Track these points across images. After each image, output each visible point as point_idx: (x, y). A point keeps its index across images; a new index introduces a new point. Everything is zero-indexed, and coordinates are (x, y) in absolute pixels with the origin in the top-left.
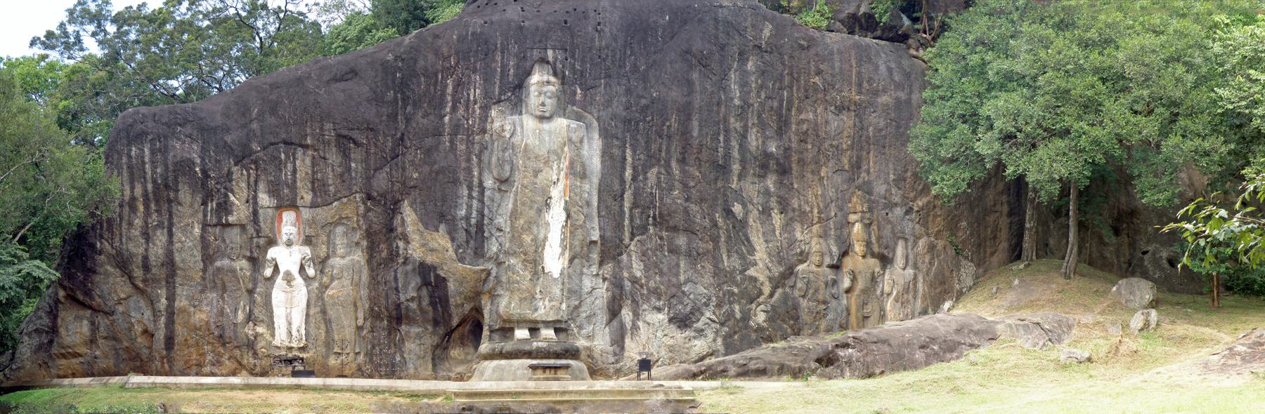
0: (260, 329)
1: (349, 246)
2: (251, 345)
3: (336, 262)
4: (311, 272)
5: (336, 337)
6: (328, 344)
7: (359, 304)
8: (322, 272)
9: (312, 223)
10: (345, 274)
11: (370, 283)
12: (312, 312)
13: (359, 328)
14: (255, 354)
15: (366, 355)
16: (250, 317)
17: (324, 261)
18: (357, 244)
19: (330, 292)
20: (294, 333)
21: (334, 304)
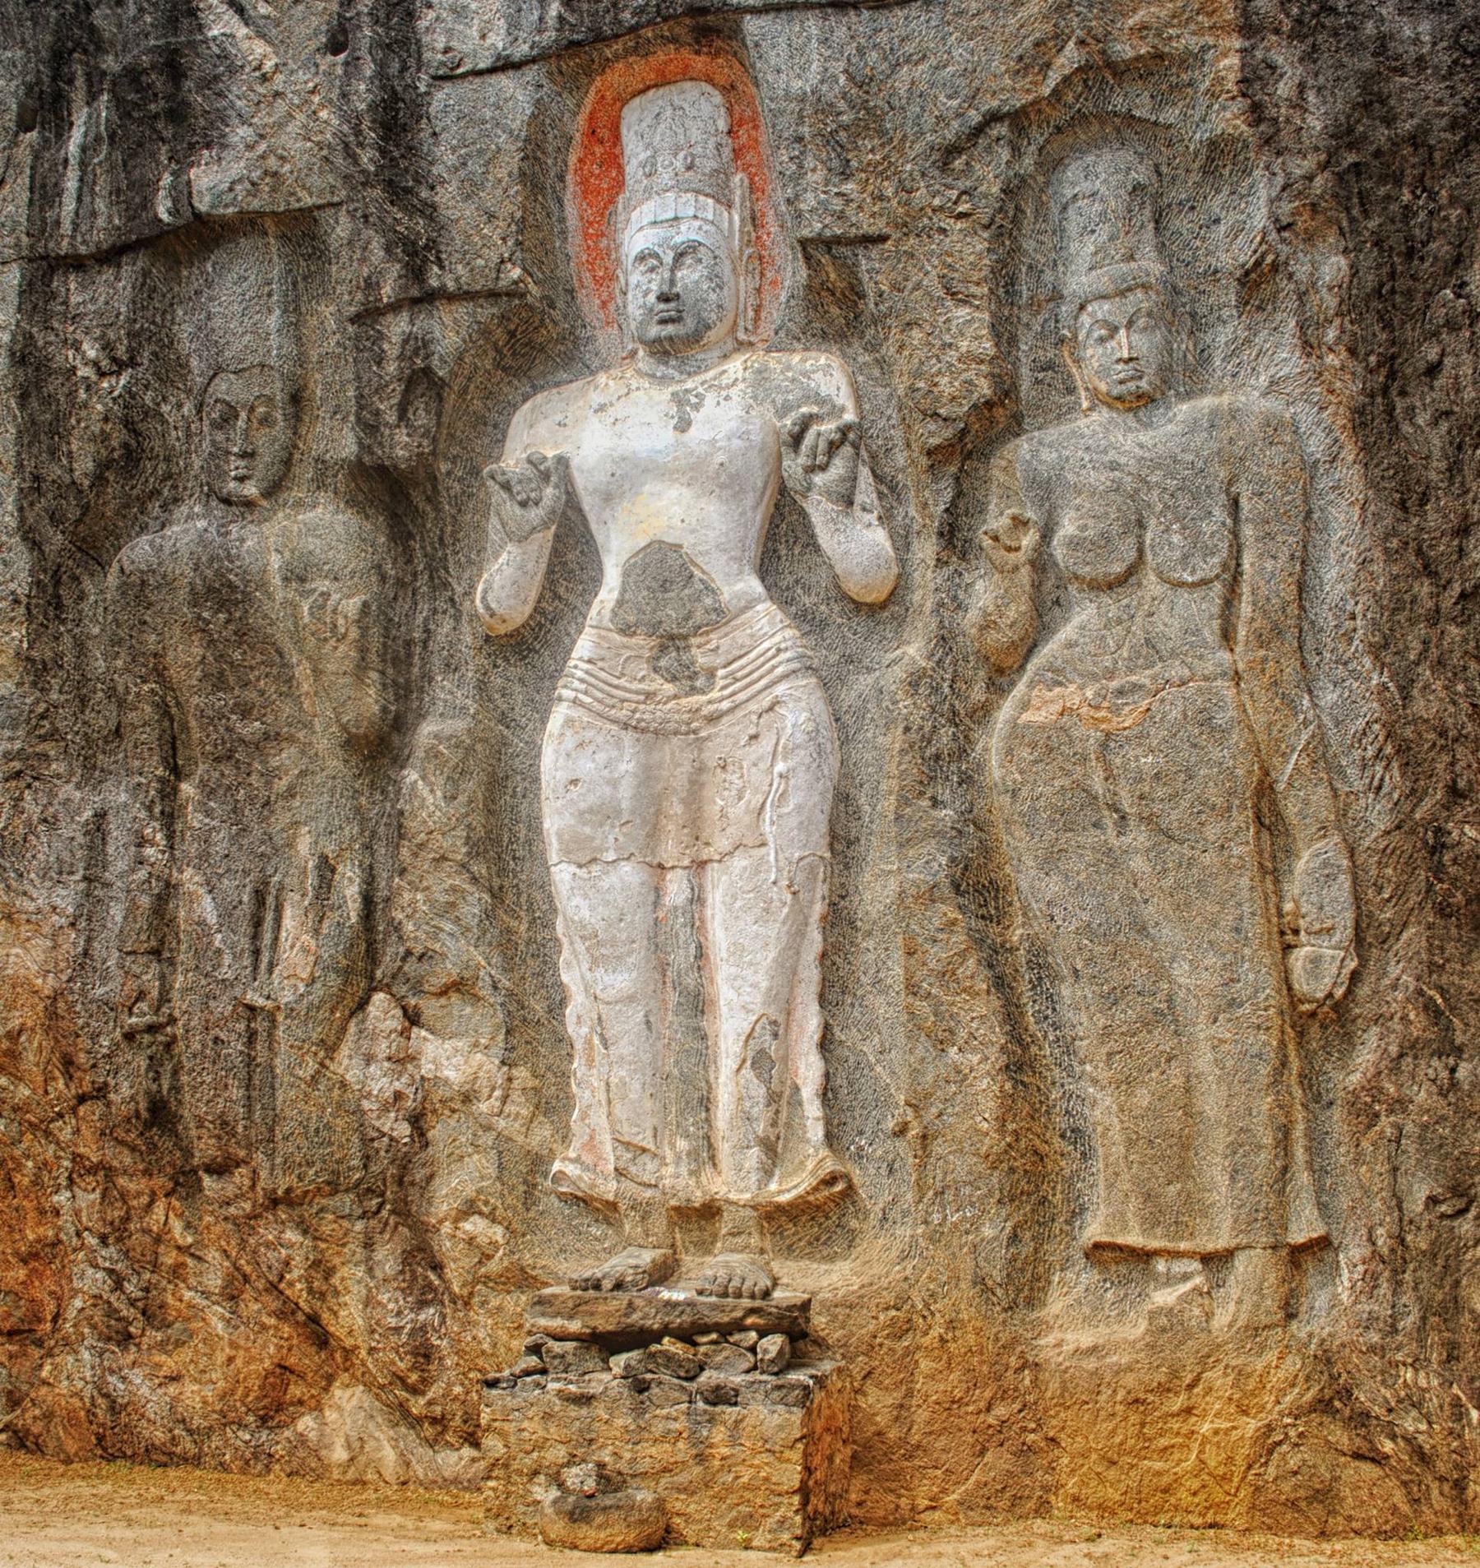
0: (452, 1057)
1: (1178, 309)
2: (390, 1188)
3: (1084, 448)
4: (856, 544)
5: (1103, 1111)
6: (1033, 1174)
7: (1306, 803)
8: (955, 538)
9: (852, 126)
10: (1166, 543)
11: (1398, 604)
12: (876, 893)
13: (1317, 1026)
14: (422, 1257)
15: (1393, 1262)
16: (368, 961)
17: (971, 444)
18: (1257, 282)
19: (1029, 705)
20: (730, 1084)
21: (1081, 809)
